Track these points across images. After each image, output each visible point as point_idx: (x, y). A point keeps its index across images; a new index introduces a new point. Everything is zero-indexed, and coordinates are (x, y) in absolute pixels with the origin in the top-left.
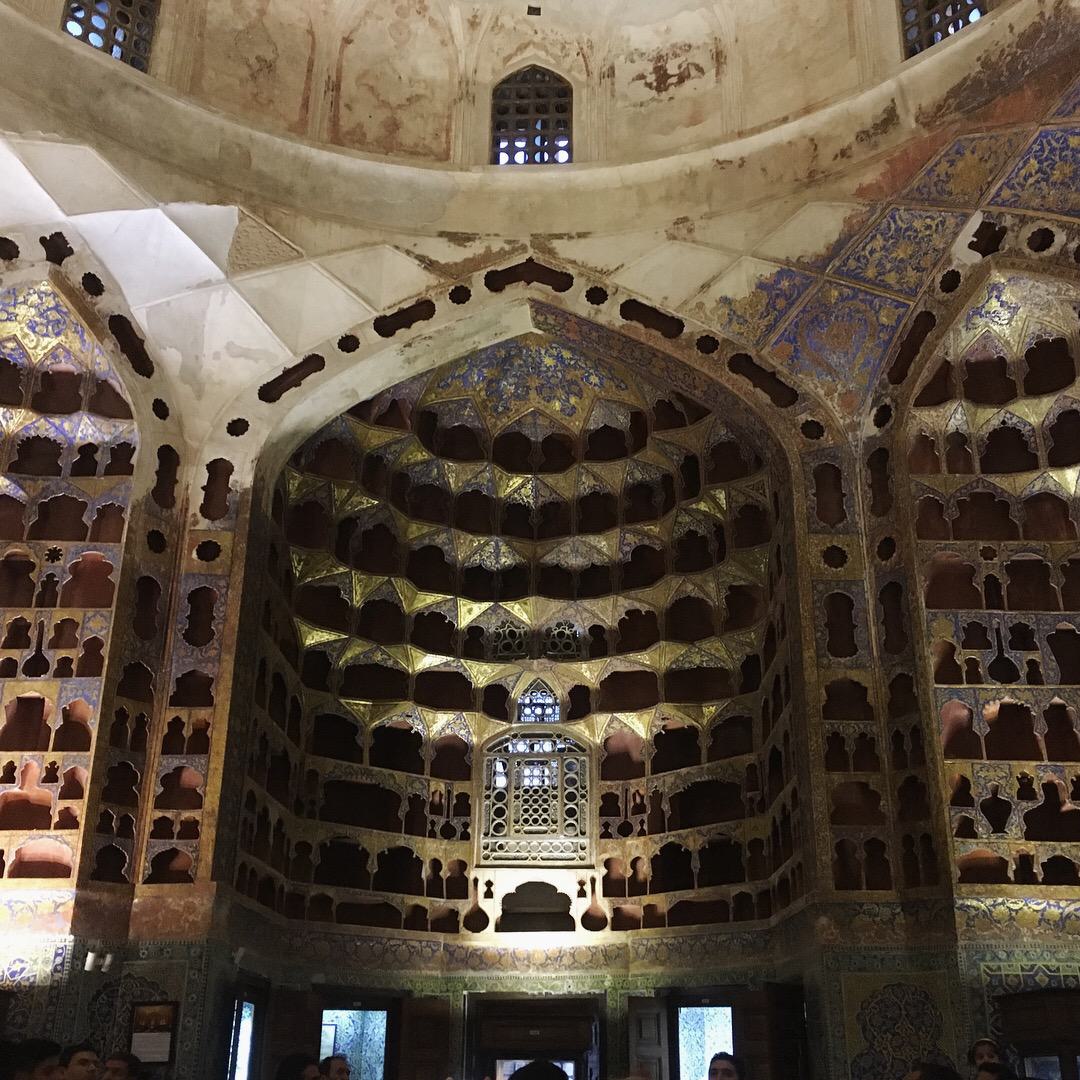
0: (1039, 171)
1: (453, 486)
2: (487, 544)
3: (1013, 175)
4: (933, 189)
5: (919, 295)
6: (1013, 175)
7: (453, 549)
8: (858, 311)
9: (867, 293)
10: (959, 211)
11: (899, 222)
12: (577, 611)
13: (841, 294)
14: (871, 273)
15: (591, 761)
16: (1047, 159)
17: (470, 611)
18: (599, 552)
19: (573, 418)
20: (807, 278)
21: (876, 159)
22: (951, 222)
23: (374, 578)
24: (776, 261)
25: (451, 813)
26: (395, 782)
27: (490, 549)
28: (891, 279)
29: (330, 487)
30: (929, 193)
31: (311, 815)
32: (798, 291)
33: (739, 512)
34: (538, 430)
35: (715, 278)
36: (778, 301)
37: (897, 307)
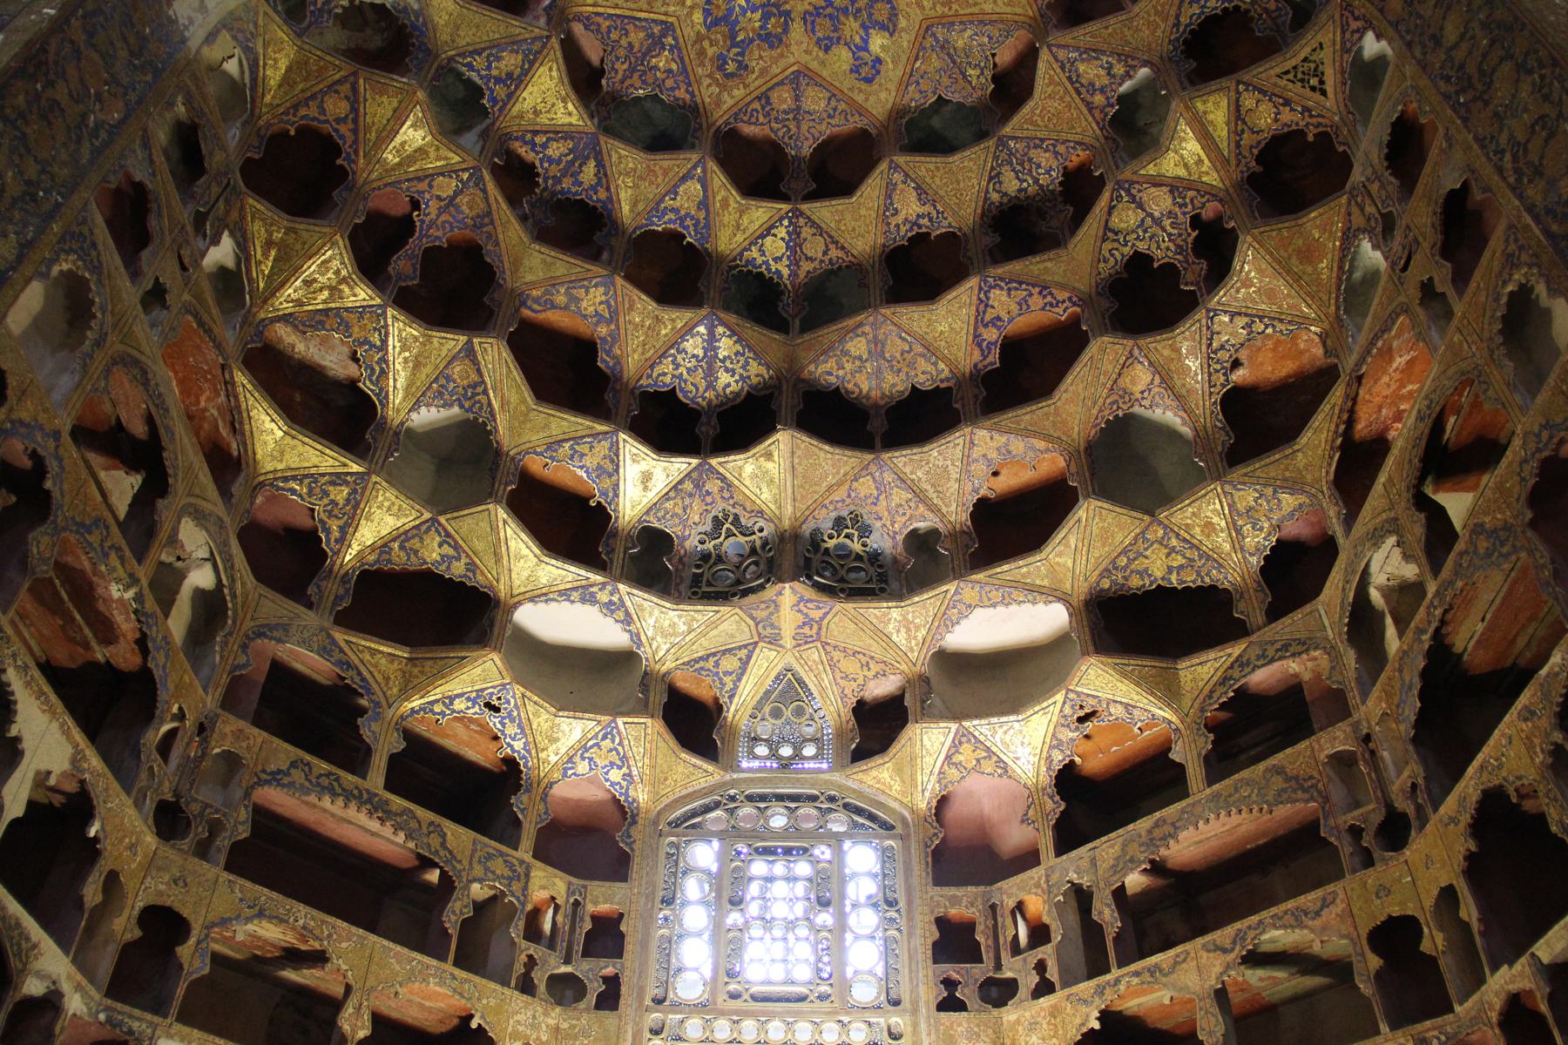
1: (626, 208)
2: (689, 330)
7: (615, 337)
12: (881, 487)
15: (907, 849)
17: (646, 478)
18: (930, 350)
19: (875, 87)
23: (437, 336)
25: (579, 947)
26: (443, 845)
27: (694, 346)
29: (355, 89)
31: (203, 850)
33: (1259, 159)
34: (804, 127)
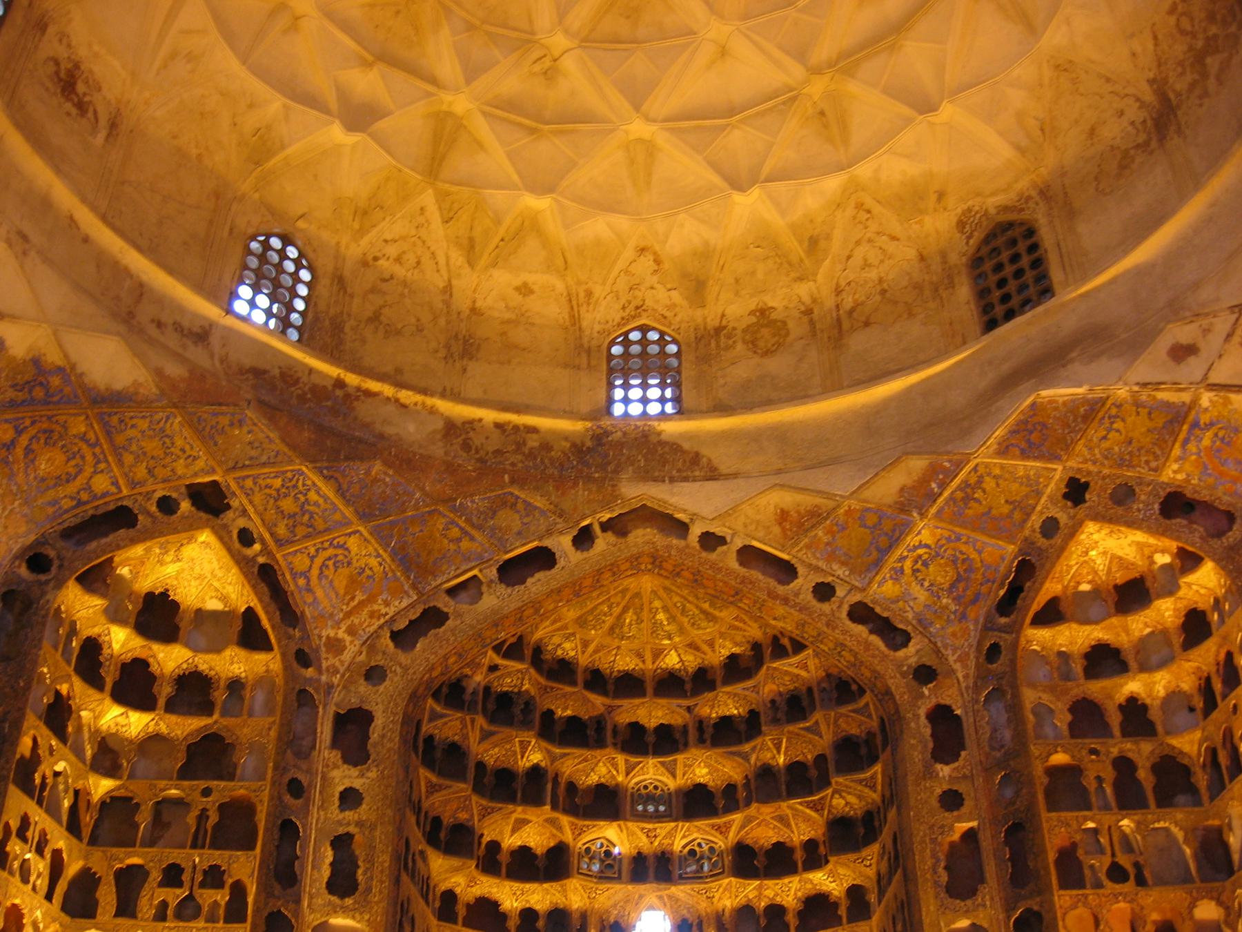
0: (278, 490)
3: (263, 476)
4: (208, 429)
5: (135, 491)
6: (263, 476)
8: (83, 457)
9: (103, 452)
10: (212, 463)
11: (168, 425)
13: (85, 433)
14: (120, 440)
16: (287, 488)
20: (76, 396)
21: (183, 360)
22: (200, 464)
24: (66, 356)
28: (128, 459)
30: (204, 429)
32: (62, 398)
35: (13, 318)
36: (38, 388)
37: (112, 484)
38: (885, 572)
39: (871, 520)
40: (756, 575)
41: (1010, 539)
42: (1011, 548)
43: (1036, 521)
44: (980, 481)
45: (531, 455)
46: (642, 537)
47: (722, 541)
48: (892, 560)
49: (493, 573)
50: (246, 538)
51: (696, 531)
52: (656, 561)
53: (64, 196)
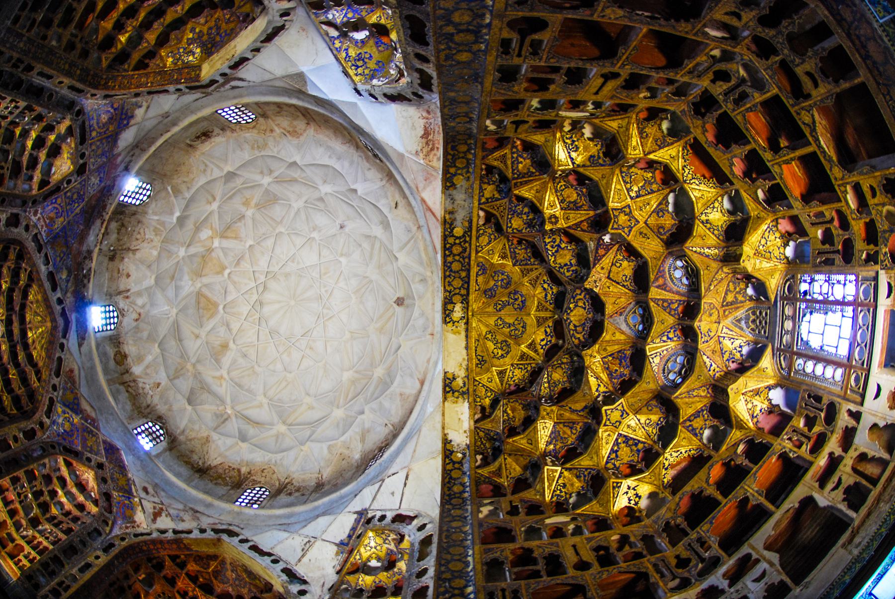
38: (64, 408)
39: (76, 401)
40: (55, 363)
41: (82, 447)
42: (80, 448)
43: (89, 455)
44: (93, 436)
45: (82, 281)
46: (61, 322)
47: (63, 351)
48: (67, 410)
49: (51, 269)
50: (69, 182)
51: (64, 341)
52: (55, 328)
53: (176, 129)
